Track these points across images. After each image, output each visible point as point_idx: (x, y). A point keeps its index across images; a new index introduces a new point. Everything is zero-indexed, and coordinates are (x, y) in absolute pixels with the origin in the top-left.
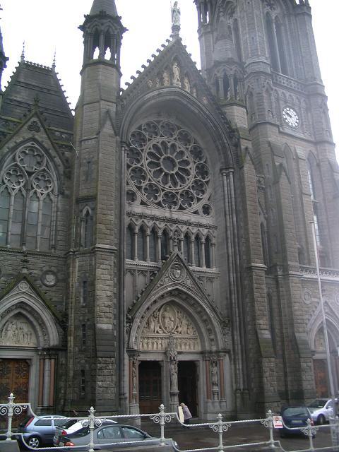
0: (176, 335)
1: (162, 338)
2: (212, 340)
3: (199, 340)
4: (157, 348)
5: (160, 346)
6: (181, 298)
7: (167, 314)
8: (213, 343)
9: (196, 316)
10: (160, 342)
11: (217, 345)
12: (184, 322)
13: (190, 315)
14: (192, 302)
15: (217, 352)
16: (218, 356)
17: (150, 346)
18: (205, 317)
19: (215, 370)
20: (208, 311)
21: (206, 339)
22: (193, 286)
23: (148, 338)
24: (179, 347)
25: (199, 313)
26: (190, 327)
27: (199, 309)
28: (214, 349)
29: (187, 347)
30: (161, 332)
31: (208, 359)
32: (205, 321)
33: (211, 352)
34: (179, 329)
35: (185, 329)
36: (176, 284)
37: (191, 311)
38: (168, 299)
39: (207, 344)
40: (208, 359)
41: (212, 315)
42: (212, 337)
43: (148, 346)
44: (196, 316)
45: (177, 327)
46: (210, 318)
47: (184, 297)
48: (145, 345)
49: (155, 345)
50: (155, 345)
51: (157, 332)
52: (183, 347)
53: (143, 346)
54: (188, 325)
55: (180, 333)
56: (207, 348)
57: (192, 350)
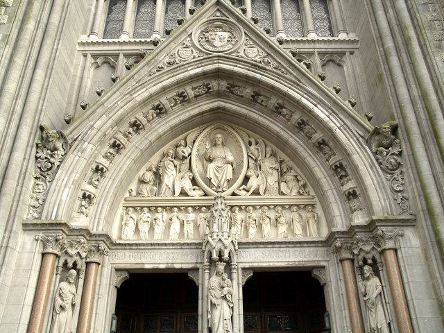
0: (244, 197)
1: (197, 209)
2: (352, 195)
3: (319, 210)
4: (182, 233)
5: (189, 228)
6: (241, 99)
7: (218, 152)
8: (355, 203)
9: (294, 140)
10: (192, 216)
11: (369, 210)
12: (268, 164)
13: (282, 144)
14: (274, 101)
15: (371, 227)
16: (378, 240)
17: (159, 229)
18: (318, 136)
19: (373, 286)
20: (320, 112)
21: (332, 196)
22: (266, 60)
23: (153, 209)
24: (253, 231)
25: (301, 125)
26: (289, 177)
27: (296, 117)
28: (360, 219)
29: (282, 229)
30: (197, 194)
31: (346, 255)
32: (321, 145)
33: (352, 231)
34: (253, 183)
35: (273, 179)
36: (210, 58)
37: (275, 126)
38: (206, 105)
39: (337, 209)
40: (346, 255)
41: (334, 123)
42: (350, 185)
43: (152, 228)
44: (294, 140)
45: (247, 179)
46: (330, 130)
47: (248, 92)
48: (144, 228)
49: (176, 225)
50: (176, 225)
51: (183, 193)
52: (267, 228)
53: (137, 230)
54: (282, 174)
55: (256, 193)
56: (340, 225)
57: (299, 235)
